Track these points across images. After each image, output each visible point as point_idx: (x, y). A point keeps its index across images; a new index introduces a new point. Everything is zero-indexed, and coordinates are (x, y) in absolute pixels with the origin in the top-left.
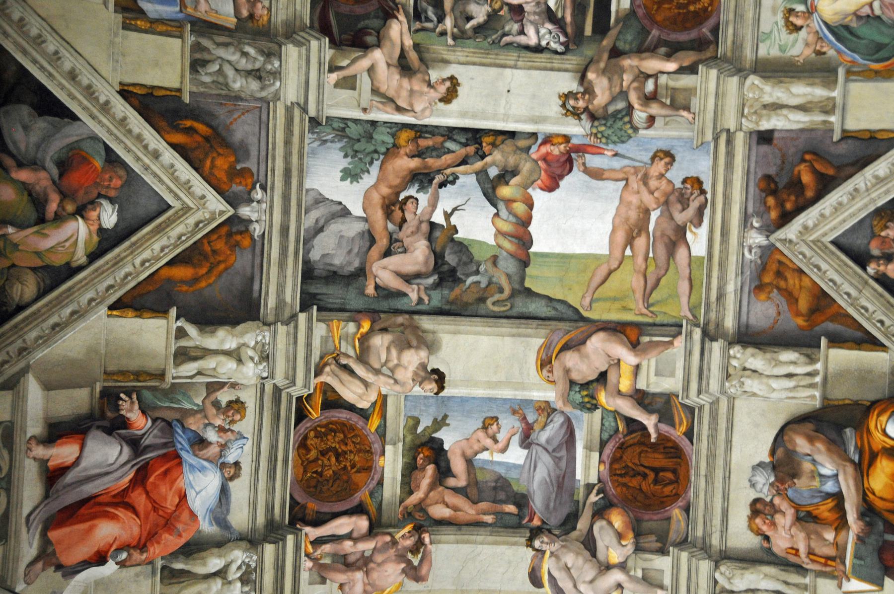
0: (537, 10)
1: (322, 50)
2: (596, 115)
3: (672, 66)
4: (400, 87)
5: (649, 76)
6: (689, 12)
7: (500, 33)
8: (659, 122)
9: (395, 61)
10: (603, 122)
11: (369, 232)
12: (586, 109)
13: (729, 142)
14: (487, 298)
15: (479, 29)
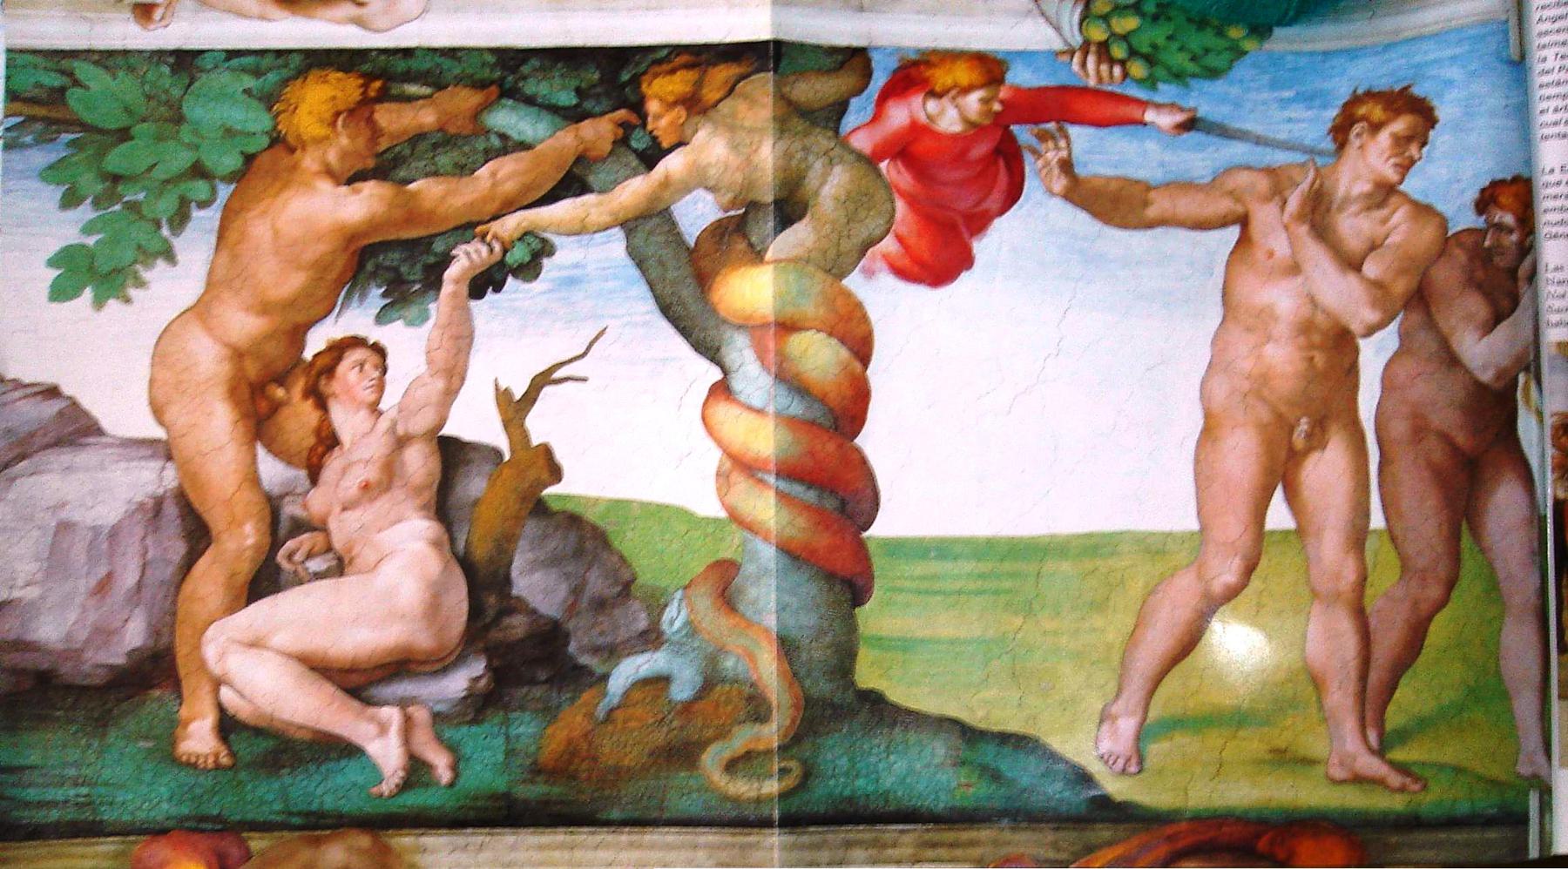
11: (181, 497)
14: (703, 745)
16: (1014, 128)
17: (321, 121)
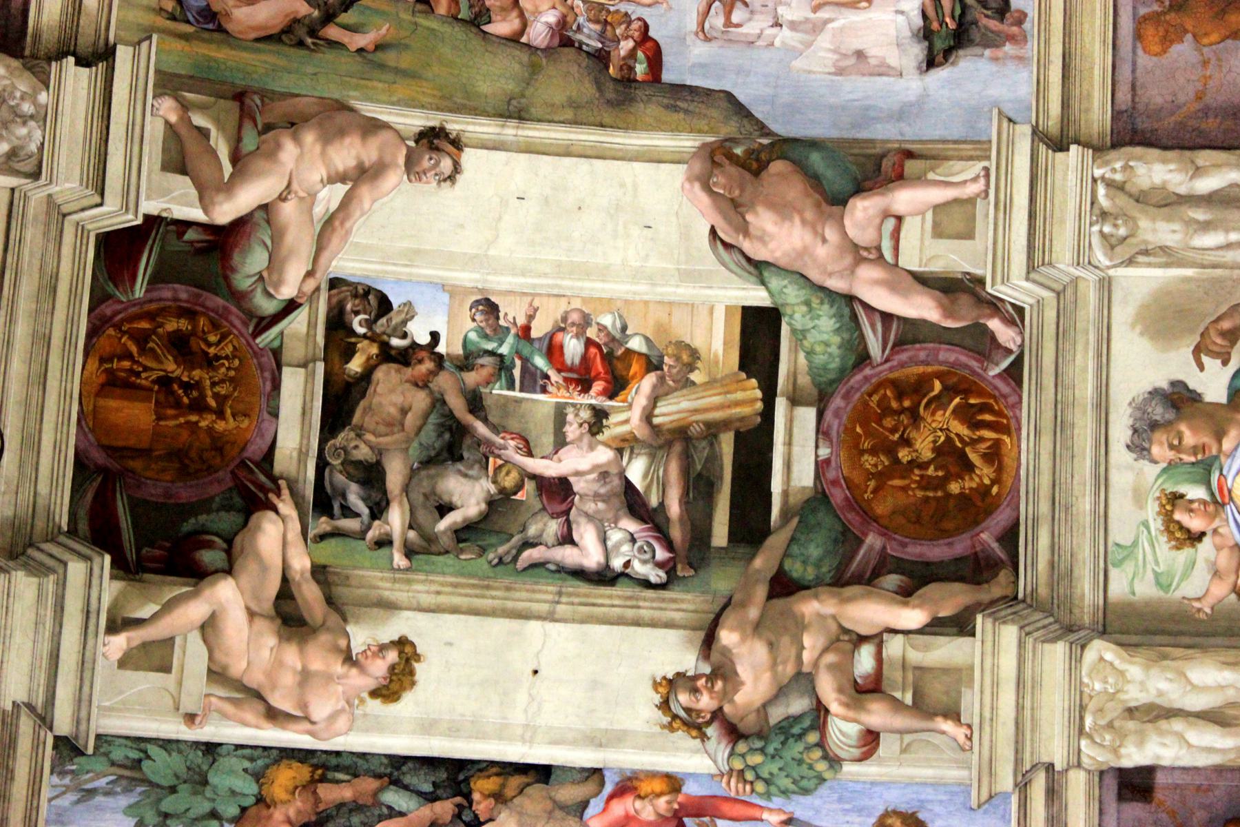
0: (603, 491)
1: (95, 582)
2: (742, 727)
3: (913, 617)
4: (279, 664)
5: (862, 639)
6: (948, 495)
7: (516, 539)
8: (888, 746)
9: (267, 605)
10: (759, 744)
12: (717, 714)
13: (1053, 793)
15: (466, 533)
16: (686, 820)
17: (287, 791)
